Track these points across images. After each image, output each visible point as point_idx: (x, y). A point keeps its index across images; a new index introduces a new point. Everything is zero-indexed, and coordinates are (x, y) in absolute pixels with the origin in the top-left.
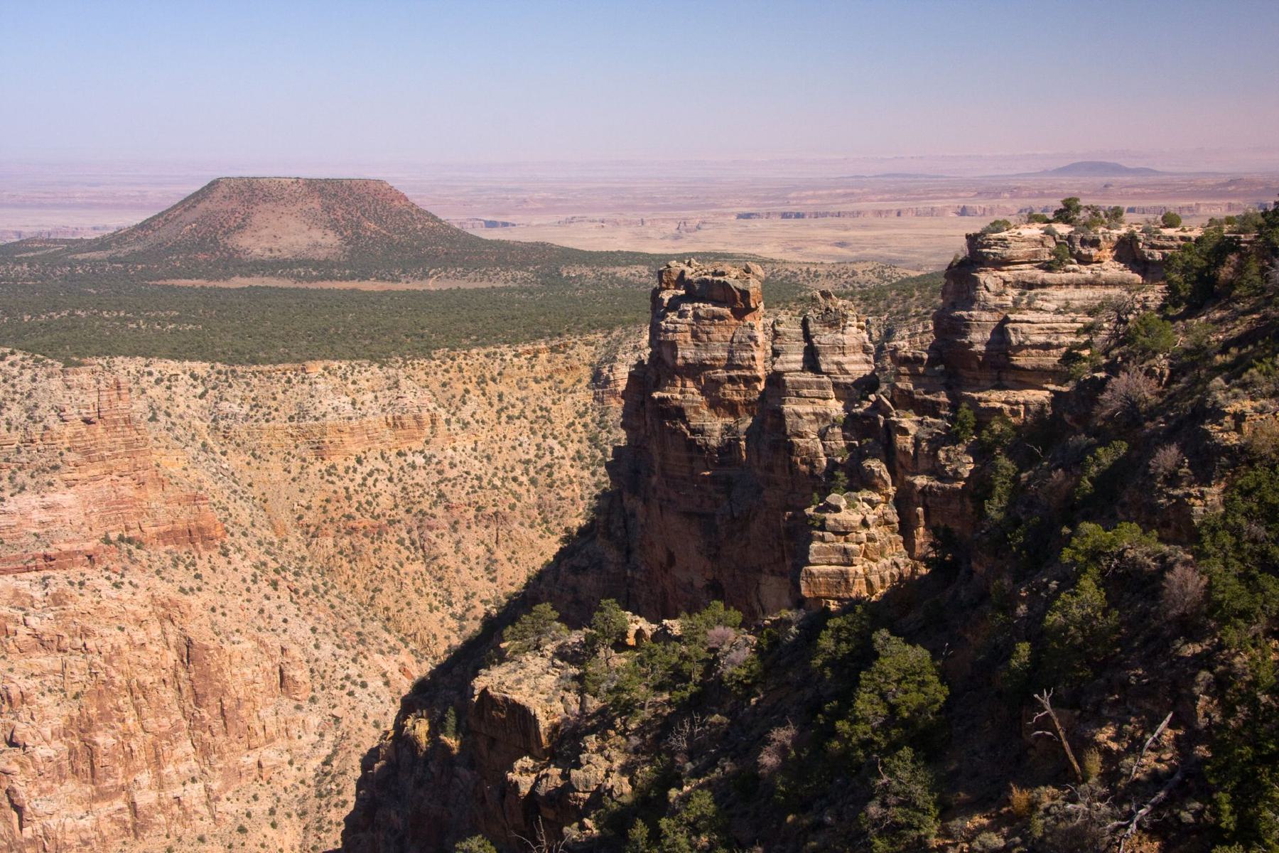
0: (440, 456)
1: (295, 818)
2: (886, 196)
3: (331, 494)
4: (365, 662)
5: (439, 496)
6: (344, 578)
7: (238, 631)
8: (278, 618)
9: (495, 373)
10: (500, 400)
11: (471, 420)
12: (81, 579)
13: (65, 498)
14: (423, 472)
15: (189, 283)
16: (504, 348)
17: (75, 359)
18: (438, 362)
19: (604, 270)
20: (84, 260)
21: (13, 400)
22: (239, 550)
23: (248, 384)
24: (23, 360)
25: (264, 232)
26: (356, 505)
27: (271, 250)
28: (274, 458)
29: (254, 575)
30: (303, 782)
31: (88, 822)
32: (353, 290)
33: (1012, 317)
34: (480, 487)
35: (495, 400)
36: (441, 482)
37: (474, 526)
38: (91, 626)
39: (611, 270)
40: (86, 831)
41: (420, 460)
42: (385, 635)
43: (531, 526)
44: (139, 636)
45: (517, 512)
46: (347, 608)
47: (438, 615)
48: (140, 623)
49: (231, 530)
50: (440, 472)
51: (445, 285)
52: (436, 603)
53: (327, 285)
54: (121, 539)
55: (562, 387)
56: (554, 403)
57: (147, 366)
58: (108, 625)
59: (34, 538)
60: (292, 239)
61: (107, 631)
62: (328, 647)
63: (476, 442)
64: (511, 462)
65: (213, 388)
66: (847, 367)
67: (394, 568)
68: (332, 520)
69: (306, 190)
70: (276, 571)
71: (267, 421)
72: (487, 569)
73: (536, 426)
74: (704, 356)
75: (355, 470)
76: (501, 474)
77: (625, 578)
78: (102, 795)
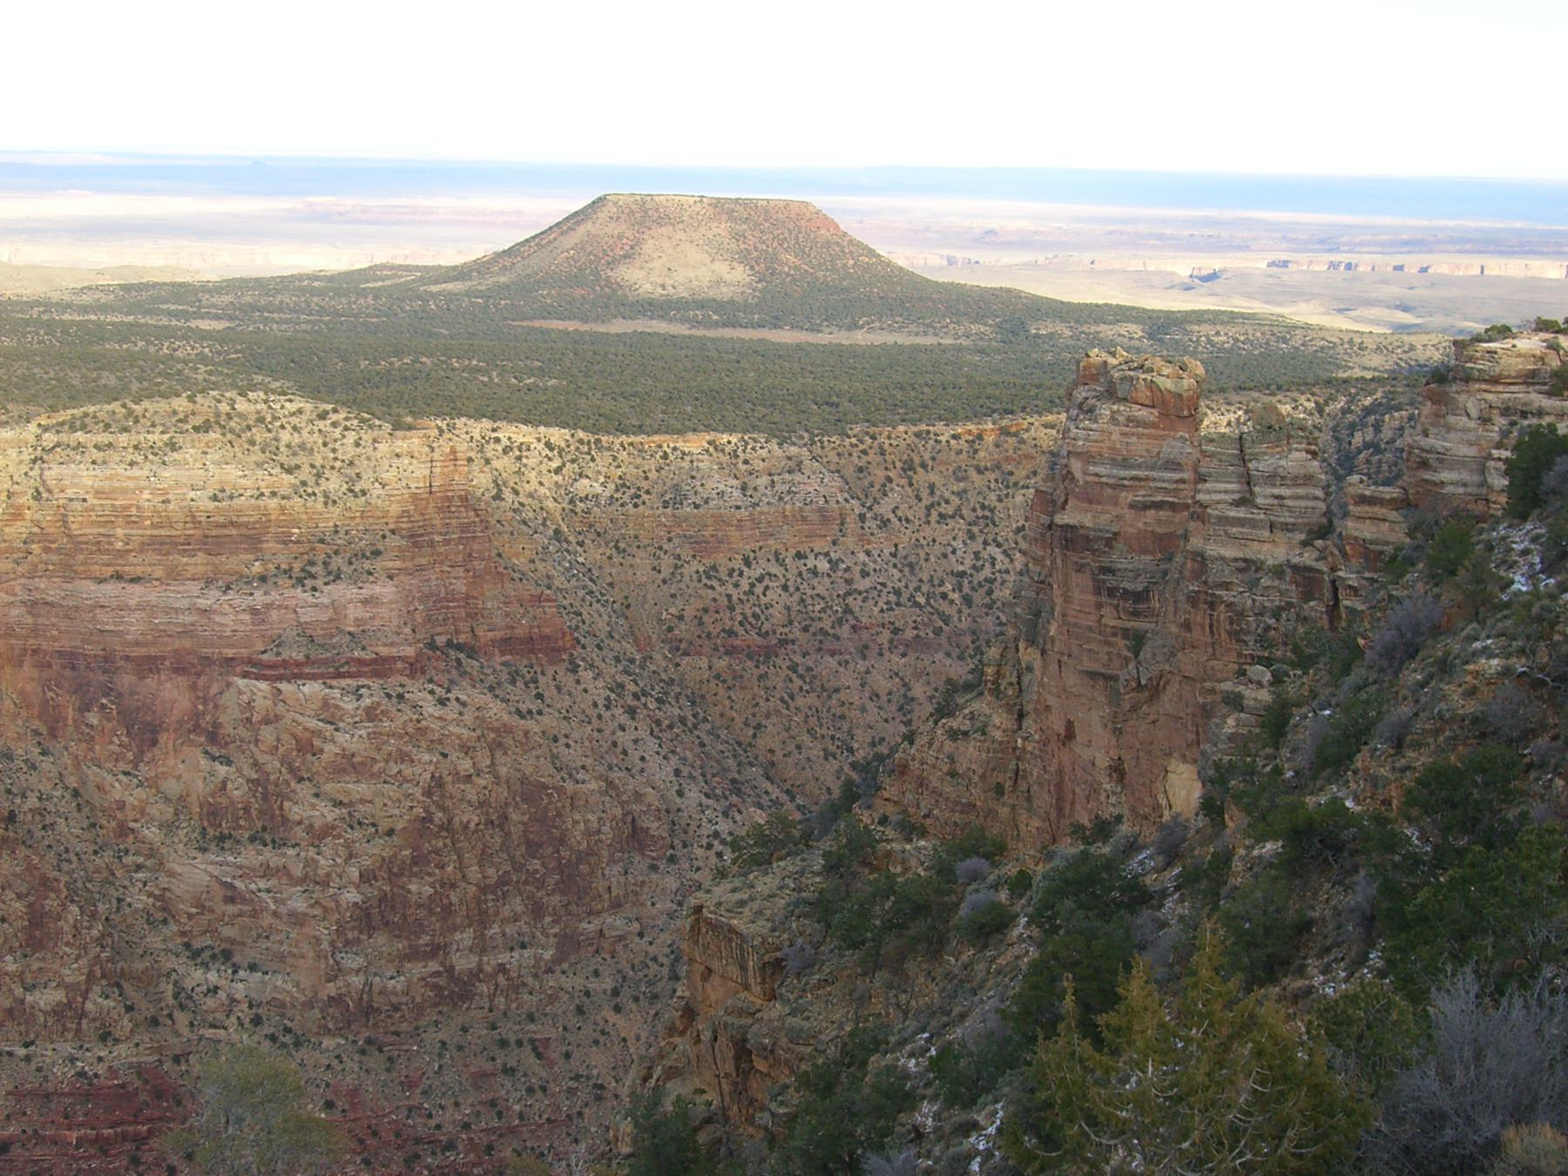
0: (849, 562)
1: (644, 1002)
2: (1467, 247)
3: (708, 602)
4: (738, 817)
5: (845, 612)
6: (718, 709)
7: (583, 767)
8: (634, 756)
9: (927, 457)
10: (932, 493)
11: (891, 516)
12: (400, 690)
13: (385, 590)
14: (827, 580)
16: (939, 427)
17: (409, 419)
18: (854, 440)
19: (1085, 328)
20: (439, 293)
21: (333, 468)
22: (592, 666)
23: (615, 458)
24: (347, 419)
26: (739, 618)
27: (663, 287)
28: (641, 553)
29: (608, 698)
30: (655, 959)
31: (398, 984)
32: (761, 341)
34: (898, 604)
35: (925, 494)
36: (848, 594)
37: (887, 654)
39: (1093, 329)
40: (395, 994)
41: (823, 566)
42: (768, 785)
43: (961, 658)
44: (465, 765)
45: (943, 639)
46: (720, 747)
47: (836, 764)
48: (466, 749)
49: (583, 640)
50: (849, 582)
51: (879, 338)
52: (832, 748)
53: (728, 333)
54: (449, 644)
55: (1012, 479)
56: (1000, 500)
57: (494, 430)
58: (429, 750)
59: (348, 638)
60: (691, 275)
61: (426, 757)
62: (693, 795)
63: (896, 546)
64: (940, 574)
65: (573, 461)
66: (1289, 502)
67: (782, 700)
68: (709, 636)
69: (711, 211)
70: (636, 696)
71: (636, 506)
72: (901, 709)
73: (975, 529)
74: (1122, 473)
75: (741, 574)
76: (925, 589)
77: (1015, 749)
78: (414, 955)
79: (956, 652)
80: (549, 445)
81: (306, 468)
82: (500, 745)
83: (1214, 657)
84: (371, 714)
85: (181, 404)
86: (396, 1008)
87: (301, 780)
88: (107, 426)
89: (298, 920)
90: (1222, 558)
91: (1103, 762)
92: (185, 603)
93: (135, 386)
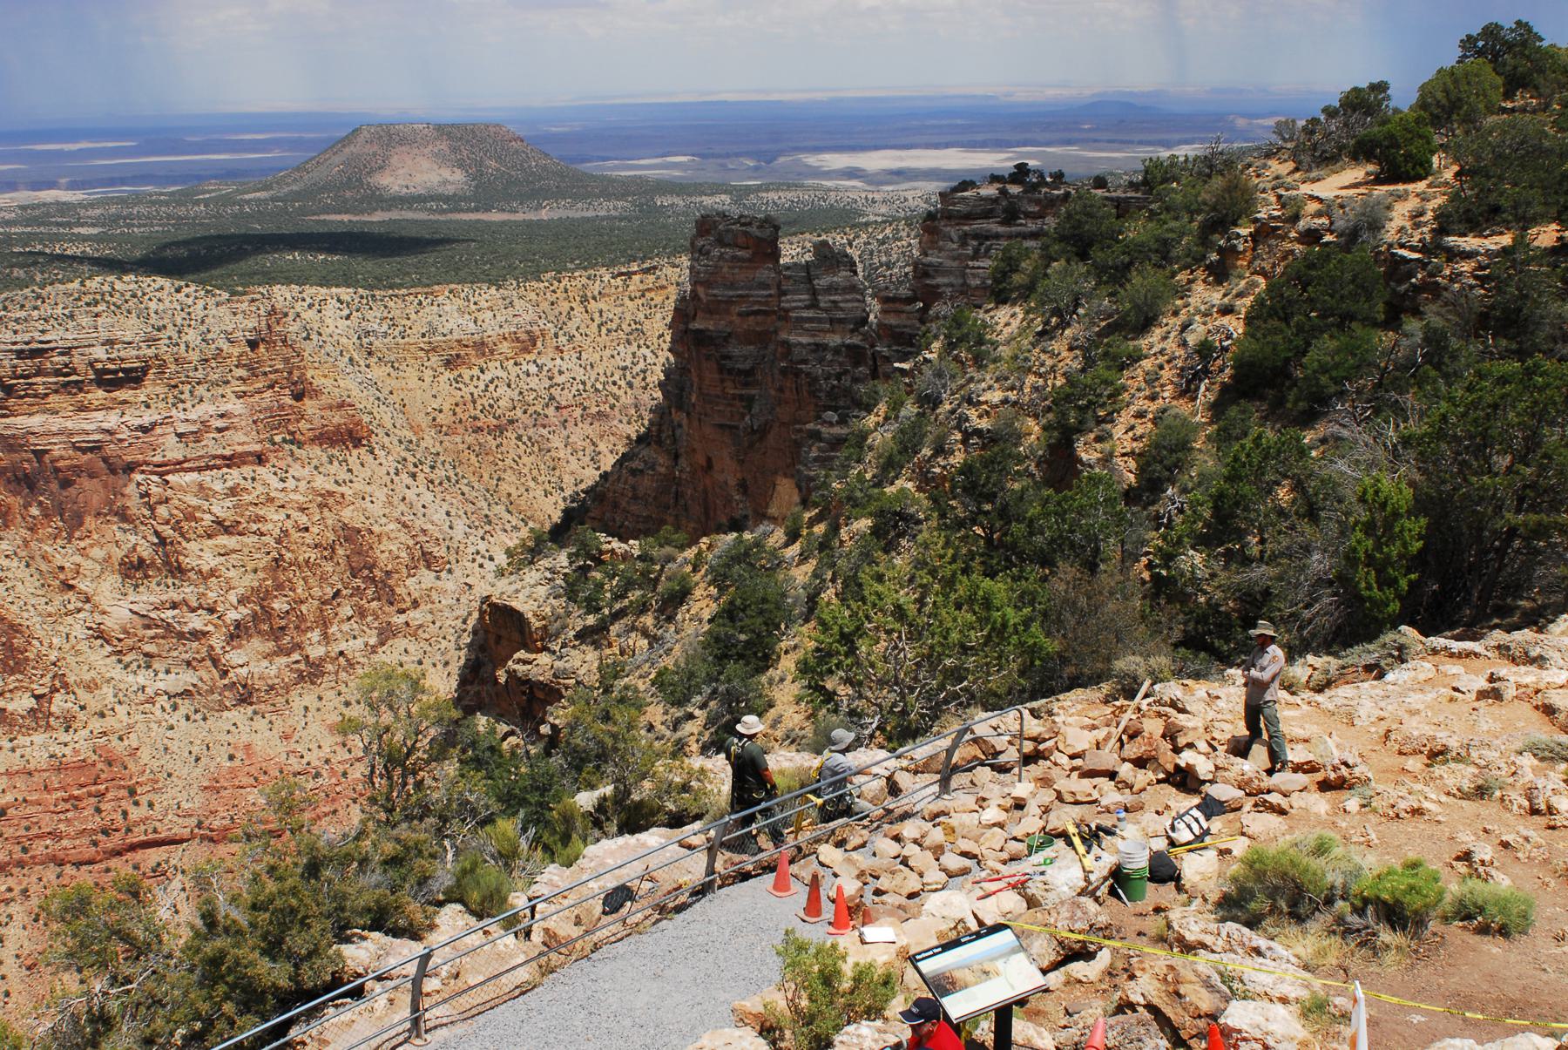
0: (550, 365)
1: (440, 666)
3: (458, 399)
13: (235, 406)
15: (338, 217)
25: (401, 172)
32: (478, 221)
33: (971, 263)
35: (596, 316)
38: (261, 513)
42: (508, 517)
47: (551, 499)
50: (551, 379)
51: (556, 215)
54: (284, 440)
60: (425, 178)
62: (460, 527)
79: (625, 420)
80: (339, 300)
81: (170, 326)
82: (326, 505)
83: (800, 408)
84: (233, 492)
85: (76, 285)
86: (272, 688)
87: (189, 540)
88: (23, 306)
89: (197, 635)
90: (800, 344)
91: (732, 482)
92: (92, 427)
93: (38, 278)
